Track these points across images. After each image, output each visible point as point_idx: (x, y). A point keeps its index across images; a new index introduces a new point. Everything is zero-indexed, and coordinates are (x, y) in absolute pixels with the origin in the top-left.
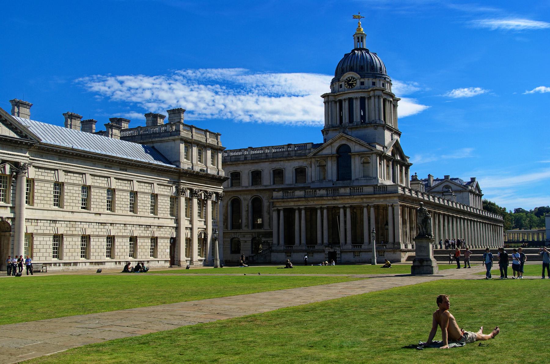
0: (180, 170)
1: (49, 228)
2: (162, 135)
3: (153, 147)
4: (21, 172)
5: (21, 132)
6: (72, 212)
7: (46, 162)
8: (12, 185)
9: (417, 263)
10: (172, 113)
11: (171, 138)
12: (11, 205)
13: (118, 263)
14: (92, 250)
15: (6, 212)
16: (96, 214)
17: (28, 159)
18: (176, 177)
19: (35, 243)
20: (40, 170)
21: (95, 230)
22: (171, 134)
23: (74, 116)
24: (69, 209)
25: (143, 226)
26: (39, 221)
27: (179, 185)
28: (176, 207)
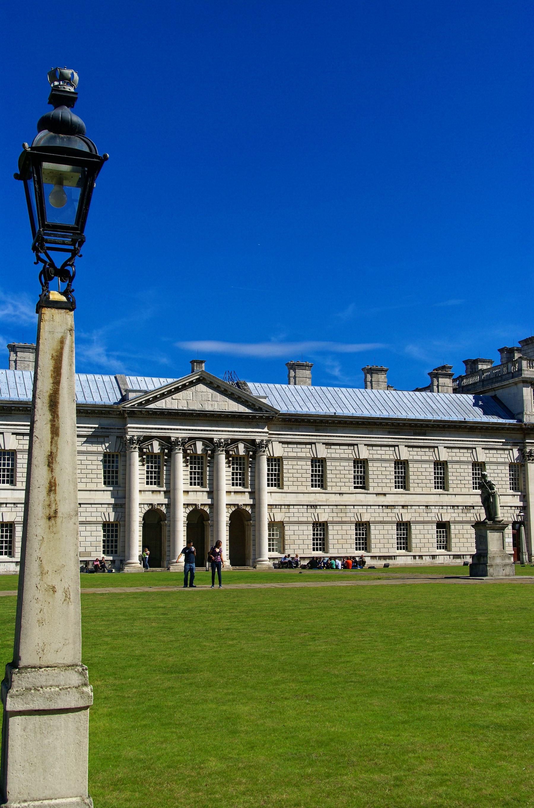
0: (521, 426)
1: (305, 515)
2: (504, 377)
3: (495, 398)
4: (259, 450)
5: (254, 405)
6: (340, 494)
7: (296, 435)
8: (250, 467)
9: (476, 561)
10: (525, 344)
11: (511, 381)
12: (249, 490)
13: (417, 557)
14: (373, 541)
15: (244, 498)
16: (377, 494)
17: (267, 435)
18: (518, 436)
19: (286, 533)
20: (290, 446)
21: (377, 515)
22: (513, 375)
23: (374, 370)
24: (335, 490)
25: (460, 508)
26: (291, 507)
27: (525, 447)
28: (522, 478)
